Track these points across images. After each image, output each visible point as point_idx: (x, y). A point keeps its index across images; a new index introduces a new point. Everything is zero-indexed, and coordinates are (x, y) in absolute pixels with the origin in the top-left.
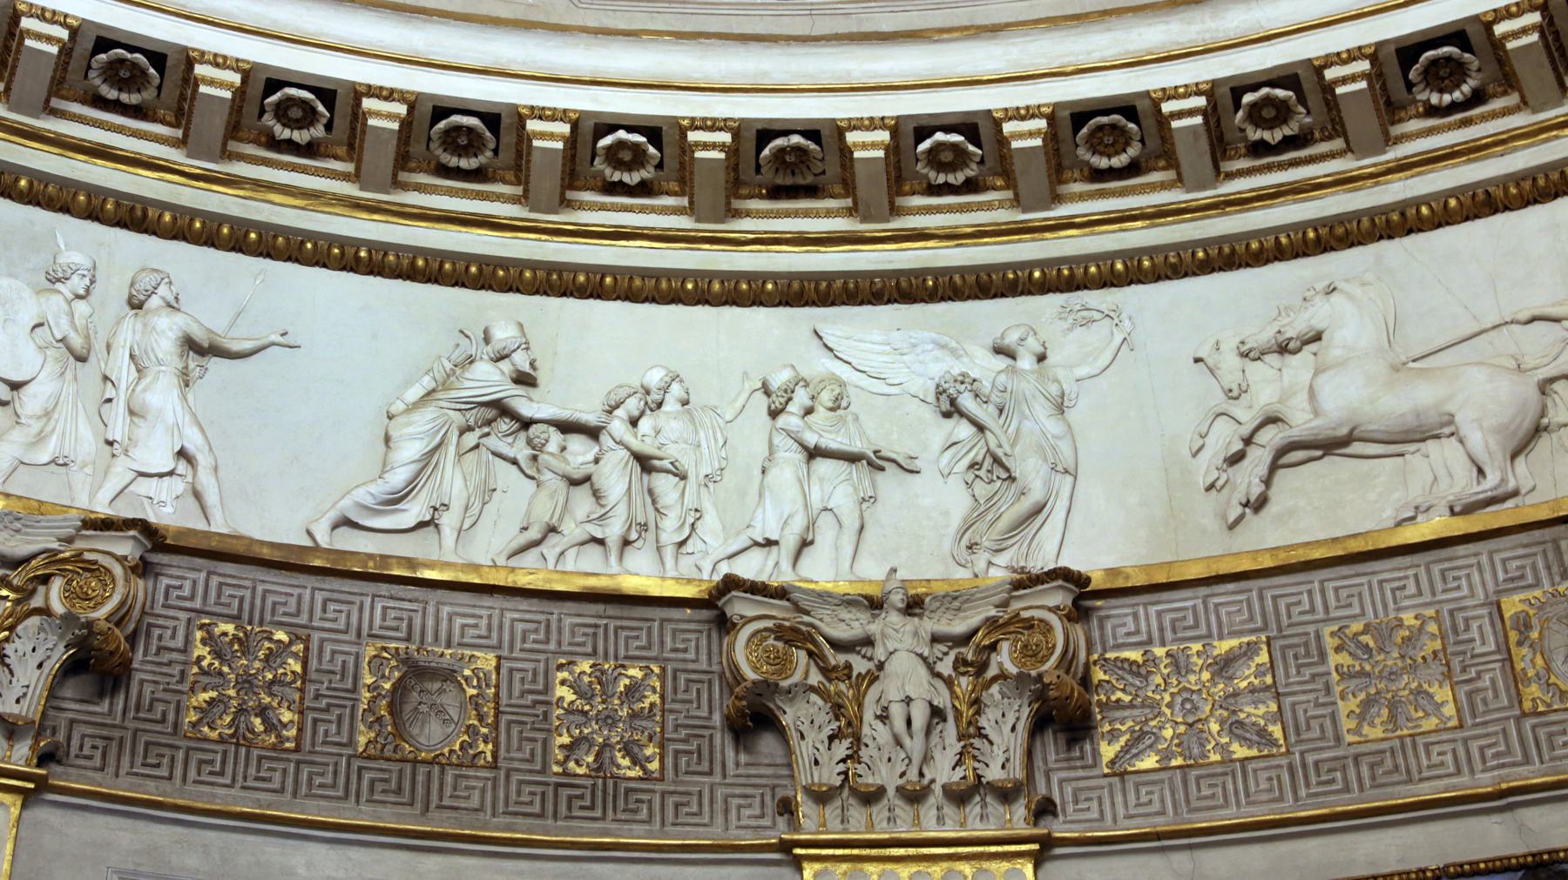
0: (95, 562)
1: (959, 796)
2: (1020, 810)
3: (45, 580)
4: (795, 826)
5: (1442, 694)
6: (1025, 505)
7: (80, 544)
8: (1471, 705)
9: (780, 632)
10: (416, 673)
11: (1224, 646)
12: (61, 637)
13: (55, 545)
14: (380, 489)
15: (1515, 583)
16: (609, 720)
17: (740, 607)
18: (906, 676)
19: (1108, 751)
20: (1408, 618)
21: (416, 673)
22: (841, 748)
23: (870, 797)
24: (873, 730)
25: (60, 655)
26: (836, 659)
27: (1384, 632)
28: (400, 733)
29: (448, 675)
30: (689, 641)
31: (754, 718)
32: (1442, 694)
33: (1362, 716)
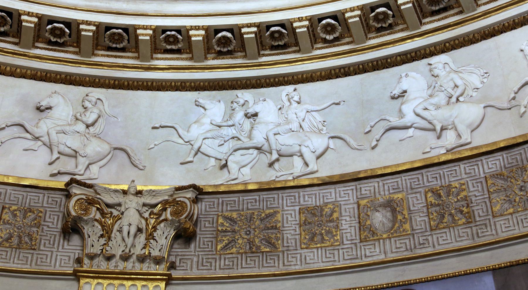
0: (180, 201)
3: (165, 209)
7: (175, 196)
12: (171, 228)
13: (166, 198)
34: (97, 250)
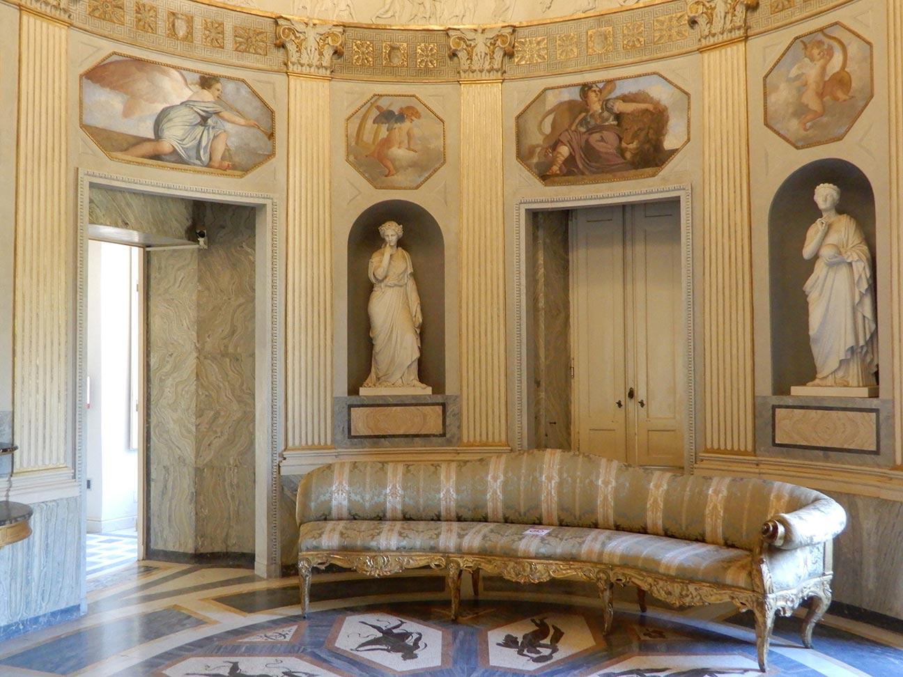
1: (489, 71)
2: (500, 73)
4: (460, 77)
5: (575, 50)
6: (506, 7)
8: (579, 54)
9: (458, 38)
10: (393, 48)
11: (539, 39)
14: (383, 10)
15: (591, 28)
16: (427, 56)
17: (451, 33)
18: (481, 48)
19: (516, 60)
20: (572, 34)
21: (393, 48)
22: (469, 62)
23: (714, 35)
24: (474, 57)
25: (332, 52)
26: (468, 43)
27: (567, 37)
28: (390, 61)
29: (398, 48)
30: (443, 40)
31: (454, 55)
32: (575, 50)
33: (561, 54)
34: (294, 59)
